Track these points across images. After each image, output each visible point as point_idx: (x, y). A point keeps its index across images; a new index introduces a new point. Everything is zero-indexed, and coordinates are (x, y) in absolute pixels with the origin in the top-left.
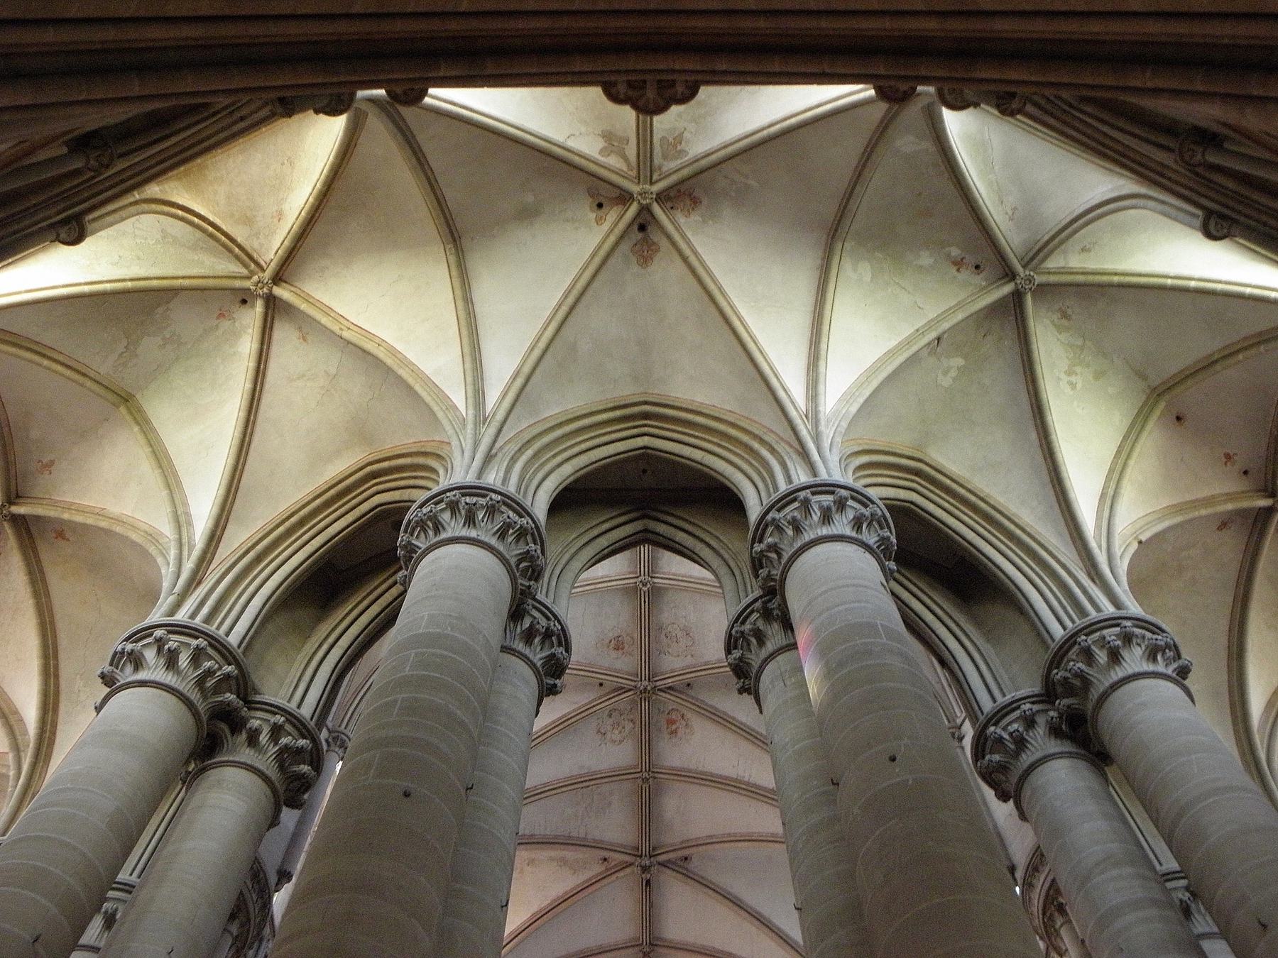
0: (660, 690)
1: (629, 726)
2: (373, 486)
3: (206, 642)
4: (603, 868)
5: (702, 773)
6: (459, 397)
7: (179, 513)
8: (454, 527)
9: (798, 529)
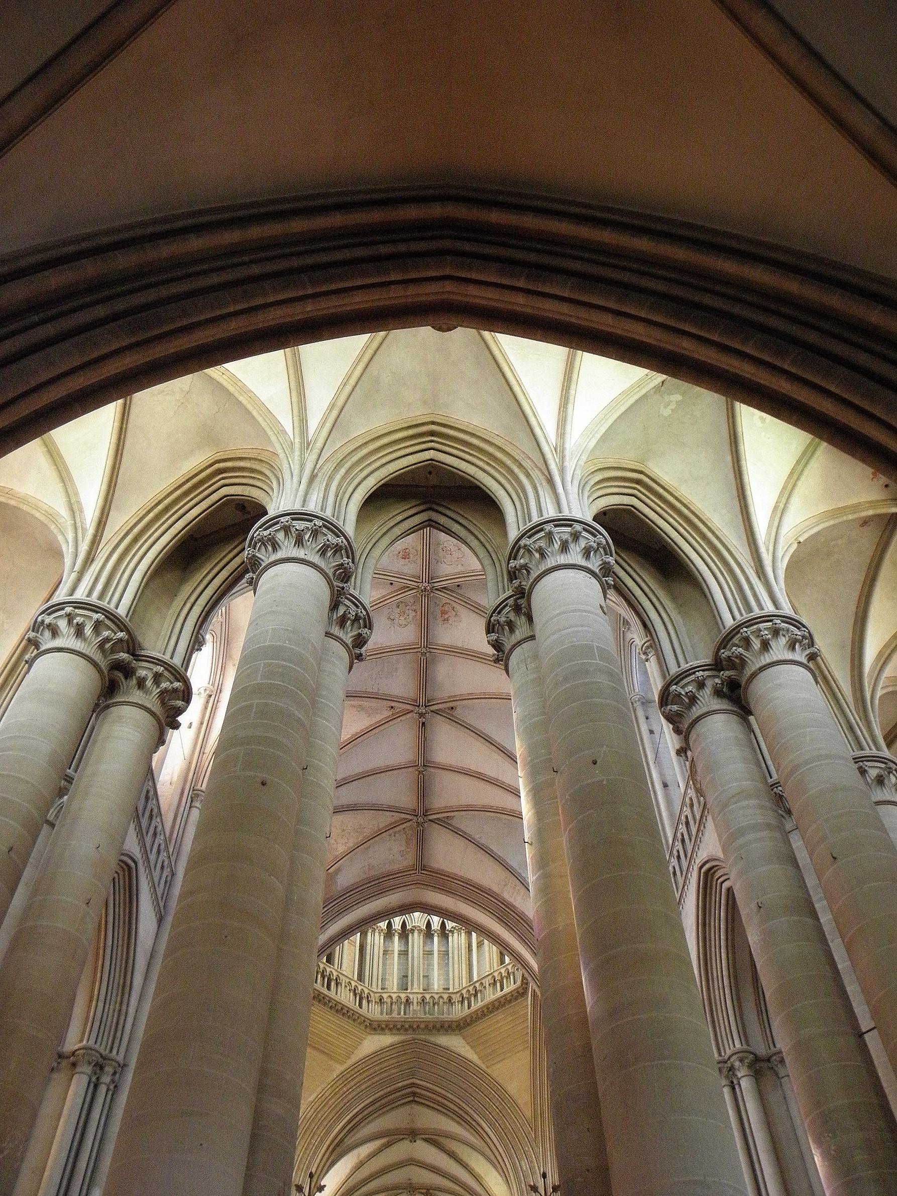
0: (436, 589)
1: (412, 614)
2: (220, 480)
3: (103, 616)
4: (391, 713)
5: (467, 650)
6: (287, 422)
7: (72, 501)
8: (288, 549)
9: (543, 555)
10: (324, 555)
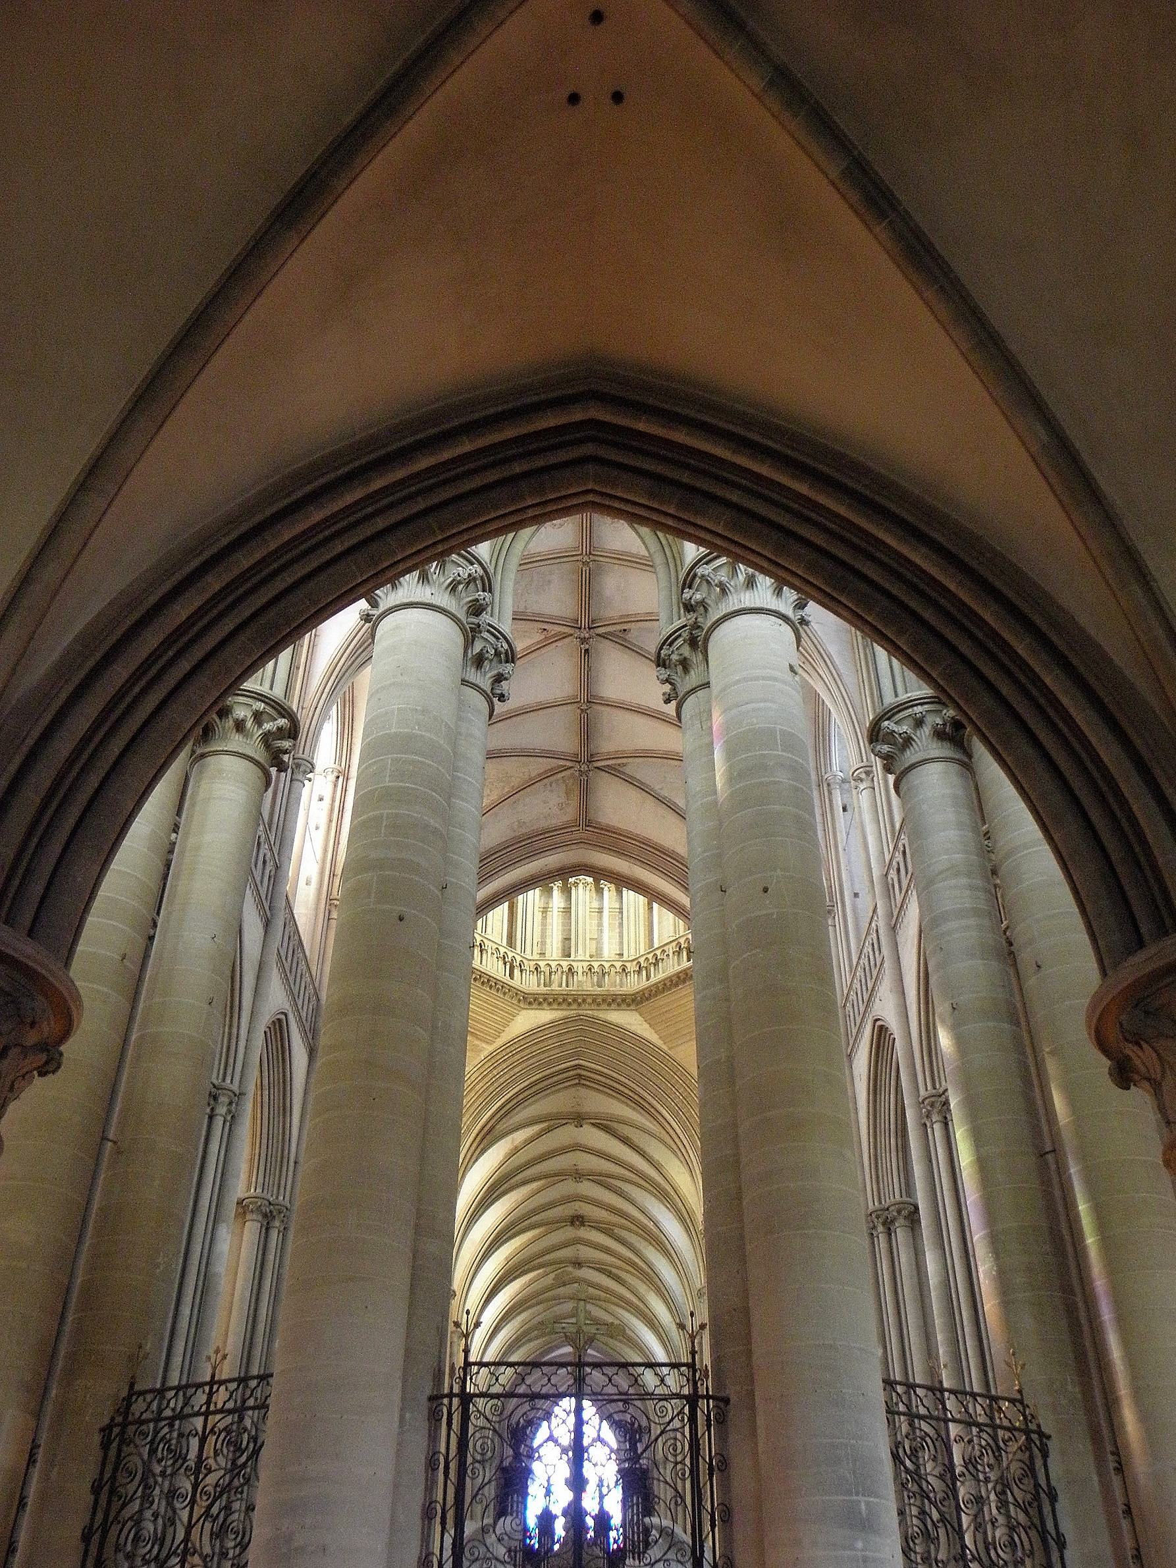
9: (724, 591)
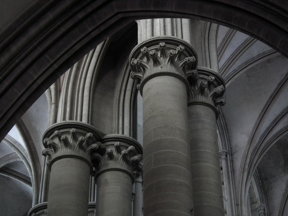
10: (173, 62)
